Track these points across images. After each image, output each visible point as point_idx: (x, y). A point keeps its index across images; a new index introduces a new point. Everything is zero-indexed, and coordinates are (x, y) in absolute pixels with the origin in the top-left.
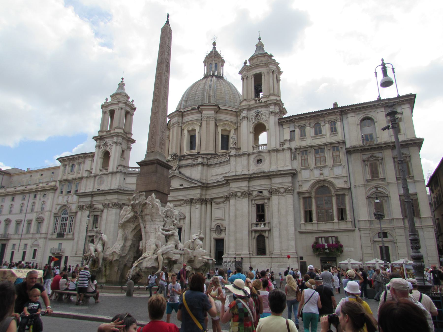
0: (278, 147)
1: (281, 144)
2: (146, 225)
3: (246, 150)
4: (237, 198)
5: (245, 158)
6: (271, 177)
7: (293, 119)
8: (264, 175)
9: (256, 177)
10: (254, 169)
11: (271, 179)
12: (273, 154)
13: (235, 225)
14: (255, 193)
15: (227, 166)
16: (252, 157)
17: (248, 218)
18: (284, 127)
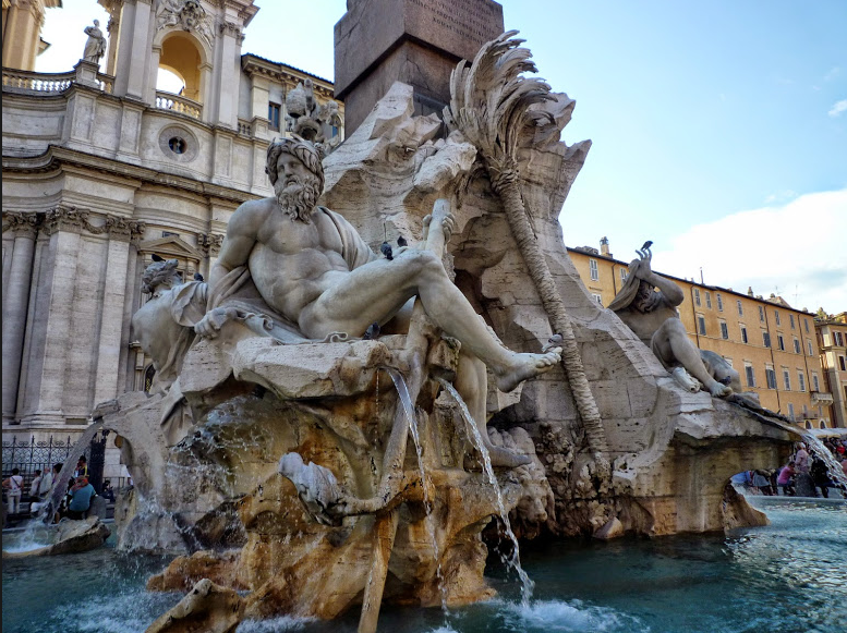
0: (235, 128)
1: (239, 125)
2: (537, 235)
3: (139, 95)
4: (87, 232)
5: (131, 118)
6: (213, 201)
7: (285, 75)
8: (200, 189)
9: (165, 186)
10: (155, 158)
11: (209, 207)
12: (222, 139)
13: (71, 321)
14: (153, 235)
15: (28, 112)
16: (156, 128)
17: (122, 305)
18: (256, 82)
